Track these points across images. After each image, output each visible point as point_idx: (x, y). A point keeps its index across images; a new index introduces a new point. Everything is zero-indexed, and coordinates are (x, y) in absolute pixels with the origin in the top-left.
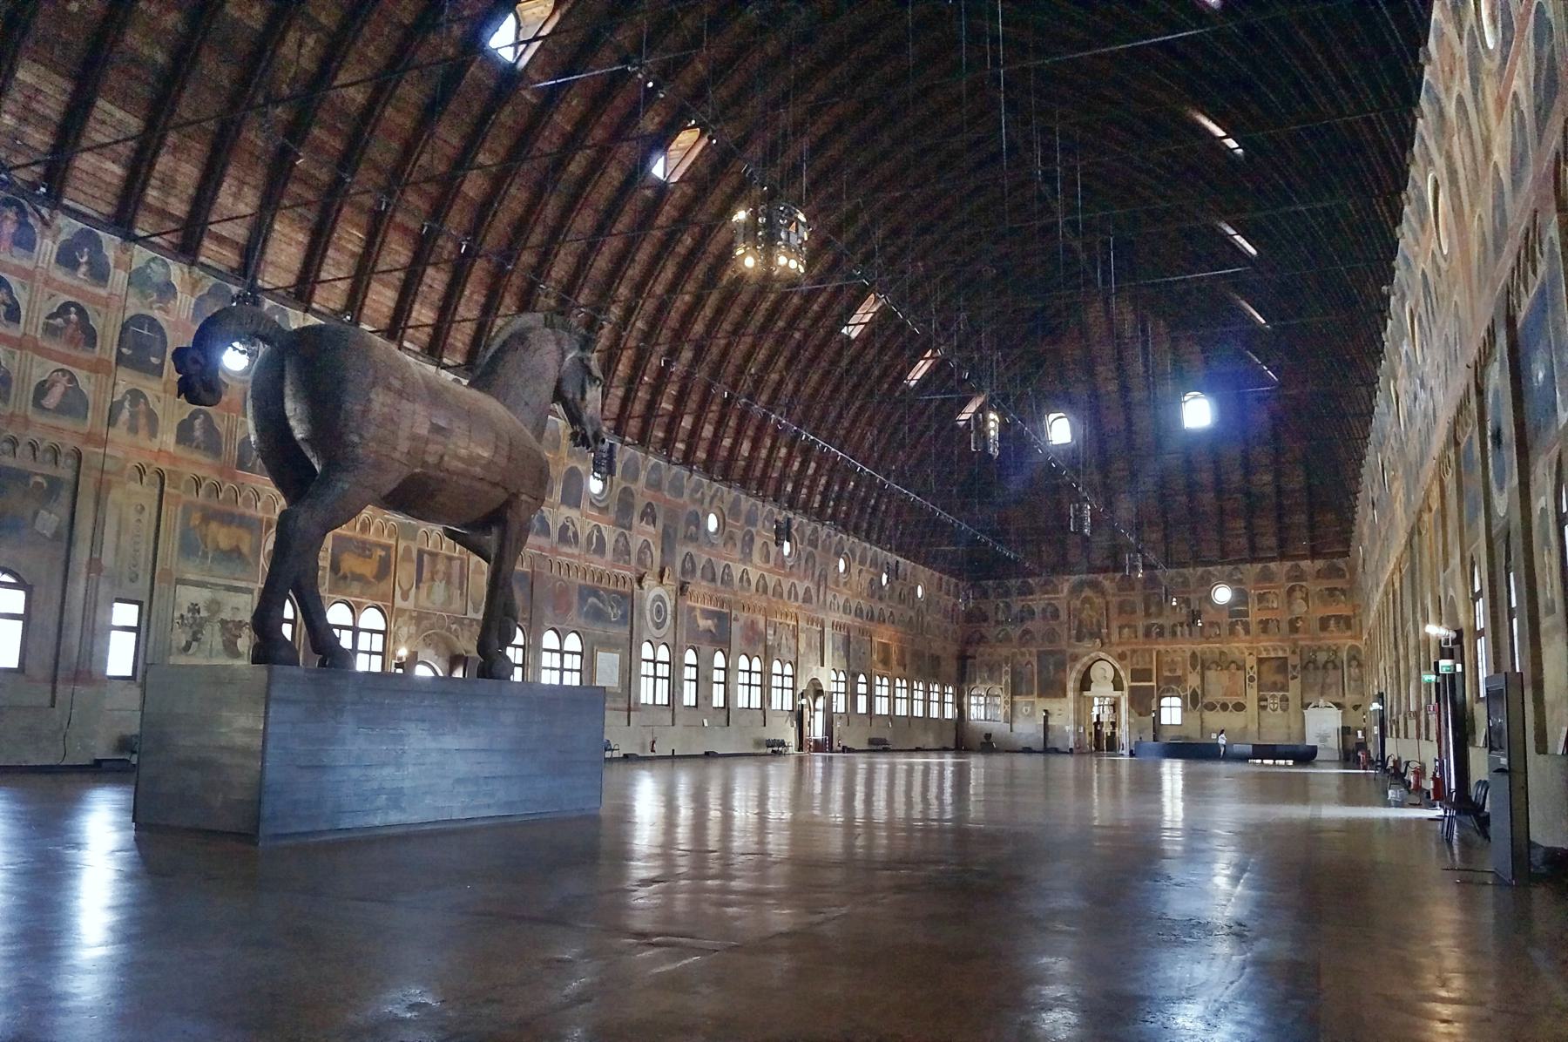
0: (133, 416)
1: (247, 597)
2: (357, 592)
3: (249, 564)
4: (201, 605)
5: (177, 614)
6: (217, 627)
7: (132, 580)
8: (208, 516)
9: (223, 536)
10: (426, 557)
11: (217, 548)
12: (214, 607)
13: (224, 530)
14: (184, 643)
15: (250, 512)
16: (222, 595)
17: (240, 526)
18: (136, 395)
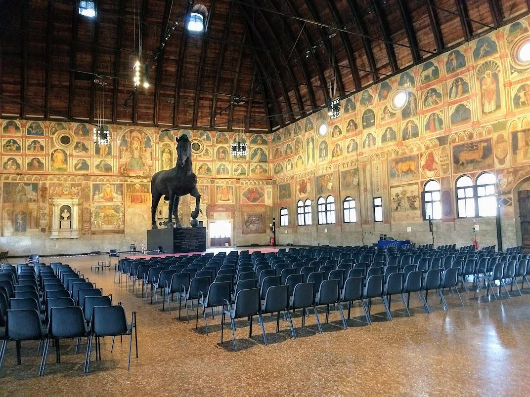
0: (369, 141)
1: (416, 186)
2: (472, 168)
3: (415, 173)
4: (400, 193)
5: (392, 198)
6: (406, 200)
7: (377, 191)
8: (397, 162)
9: (403, 167)
10: (519, 135)
11: (403, 171)
12: (404, 193)
13: (404, 164)
14: (395, 208)
15: (413, 154)
16: (406, 188)
17: (410, 160)
18: (369, 134)
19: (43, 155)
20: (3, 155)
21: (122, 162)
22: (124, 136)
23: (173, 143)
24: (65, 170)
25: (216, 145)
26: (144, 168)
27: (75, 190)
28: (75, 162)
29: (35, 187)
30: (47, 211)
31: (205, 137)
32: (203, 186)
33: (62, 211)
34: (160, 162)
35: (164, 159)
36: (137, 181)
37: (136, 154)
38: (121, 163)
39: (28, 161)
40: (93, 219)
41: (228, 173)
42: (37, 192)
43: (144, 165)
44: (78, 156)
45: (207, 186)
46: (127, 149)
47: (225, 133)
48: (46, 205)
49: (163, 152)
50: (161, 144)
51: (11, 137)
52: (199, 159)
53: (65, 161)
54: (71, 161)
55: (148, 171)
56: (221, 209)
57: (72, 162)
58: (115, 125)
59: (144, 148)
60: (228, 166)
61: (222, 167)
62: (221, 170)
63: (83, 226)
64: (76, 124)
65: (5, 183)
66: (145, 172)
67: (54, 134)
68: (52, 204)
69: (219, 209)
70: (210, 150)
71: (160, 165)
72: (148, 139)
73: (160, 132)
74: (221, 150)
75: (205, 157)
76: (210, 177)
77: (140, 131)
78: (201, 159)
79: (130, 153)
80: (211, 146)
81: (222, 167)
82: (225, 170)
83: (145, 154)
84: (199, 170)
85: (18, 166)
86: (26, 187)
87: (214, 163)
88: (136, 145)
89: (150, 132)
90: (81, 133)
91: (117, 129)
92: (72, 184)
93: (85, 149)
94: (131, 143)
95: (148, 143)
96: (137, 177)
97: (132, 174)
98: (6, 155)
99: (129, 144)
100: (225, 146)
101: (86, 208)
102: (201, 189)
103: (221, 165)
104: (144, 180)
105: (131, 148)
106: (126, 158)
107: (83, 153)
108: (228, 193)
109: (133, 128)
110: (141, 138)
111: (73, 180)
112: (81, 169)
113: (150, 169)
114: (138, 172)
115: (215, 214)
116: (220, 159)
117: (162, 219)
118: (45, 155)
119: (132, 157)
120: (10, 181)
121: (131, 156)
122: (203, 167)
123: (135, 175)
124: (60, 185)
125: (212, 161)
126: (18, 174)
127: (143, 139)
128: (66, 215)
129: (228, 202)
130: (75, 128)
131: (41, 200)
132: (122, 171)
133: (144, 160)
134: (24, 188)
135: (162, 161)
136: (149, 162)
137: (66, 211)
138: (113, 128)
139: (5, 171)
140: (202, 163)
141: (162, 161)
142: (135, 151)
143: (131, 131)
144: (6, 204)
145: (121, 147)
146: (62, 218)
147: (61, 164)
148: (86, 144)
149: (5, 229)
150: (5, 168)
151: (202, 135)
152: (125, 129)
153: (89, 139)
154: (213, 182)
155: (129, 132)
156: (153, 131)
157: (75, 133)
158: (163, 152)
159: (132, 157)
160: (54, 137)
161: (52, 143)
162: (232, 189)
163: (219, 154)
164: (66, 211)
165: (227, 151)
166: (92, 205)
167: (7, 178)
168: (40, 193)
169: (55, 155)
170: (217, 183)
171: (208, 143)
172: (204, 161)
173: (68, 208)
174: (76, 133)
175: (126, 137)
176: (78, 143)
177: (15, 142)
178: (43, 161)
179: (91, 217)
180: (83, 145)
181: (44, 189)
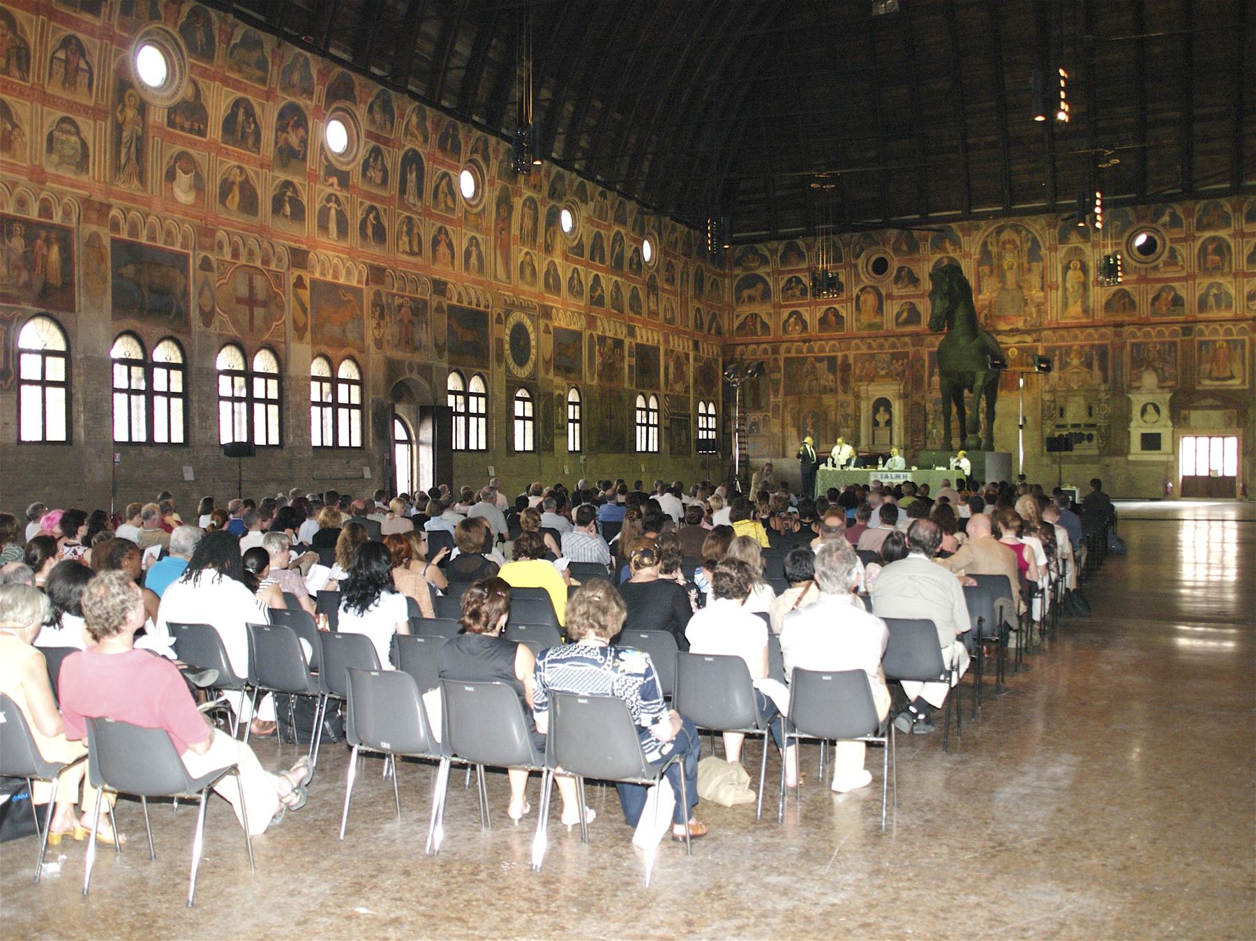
19: (842, 301)
20: (782, 307)
22: (985, 244)
23: (1089, 245)
24: (879, 327)
25: (1198, 234)
27: (898, 366)
28: (896, 309)
29: (832, 360)
30: (851, 410)
31: (1166, 218)
32: (1163, 343)
33: (876, 410)
35: (1069, 285)
36: (1010, 341)
37: (1011, 277)
39: (819, 314)
40: (929, 426)
41: (1229, 306)
42: (835, 374)
43: (1026, 304)
44: (902, 297)
45: (1173, 344)
46: (992, 272)
47: (1222, 201)
48: (850, 398)
49: (1066, 268)
50: (1063, 250)
51: (792, 271)
52: (1152, 275)
53: (879, 310)
54: (889, 309)
56: (1210, 401)
57: (892, 309)
58: (966, 223)
59: (1026, 265)
60: (1229, 285)
61: (1214, 291)
62: (1211, 300)
63: (912, 441)
64: (895, 232)
65: (786, 359)
67: (858, 256)
68: (857, 397)
69: (1203, 403)
70: (1183, 250)
71: (1060, 299)
72: (1036, 244)
73: (1060, 223)
74: (1210, 248)
75: (1168, 269)
76: (1181, 318)
77: (1016, 229)
78: (1159, 276)
80: (1185, 240)
81: (1214, 291)
82: (1223, 300)
83: (1027, 277)
84: (1153, 304)
85: (804, 323)
86: (817, 365)
87: (1191, 282)
88: (1009, 259)
89: (1038, 227)
90: (904, 248)
91: (969, 229)
92: (892, 354)
93: (914, 281)
94: (1000, 257)
95: (1034, 254)
96: (1011, 330)
97: (1003, 326)
98: (786, 306)
100: (1223, 233)
101: (917, 404)
102: (1159, 352)
103: (1211, 286)
104: (1028, 339)
105: (1000, 267)
107: (910, 290)
108: (1230, 359)
109: (1002, 222)
110: (1018, 243)
111: (893, 346)
112: (907, 322)
113: (1039, 311)
114: (1014, 319)
115: (1196, 416)
116: (1207, 271)
117: (1064, 426)
118: (845, 301)
119: (1003, 288)
120: (793, 354)
121: (1000, 285)
122: (1164, 295)
123: (1007, 328)
124: (873, 356)
125: (1185, 279)
126: (805, 341)
128: (882, 417)
129: (1230, 382)
130: (893, 240)
131: (840, 390)
133: (1026, 292)
134: (814, 367)
135: (1065, 290)
136: (1037, 294)
137: (882, 409)
138: (962, 230)
139: (787, 337)
140: (1159, 286)
141: (1065, 290)
143: (999, 231)
144: (789, 398)
146: (876, 423)
147: (872, 314)
148: (915, 268)
149: (788, 443)
150: (785, 330)
151: (1157, 215)
152: (985, 230)
153: (919, 260)
154: (1187, 331)
157: (894, 251)
158: (1066, 268)
159: (1003, 288)
160: (861, 262)
161: (857, 274)
162: (1243, 347)
163: (1205, 256)
164: (882, 409)
165: (1229, 248)
166: (928, 396)
167: (789, 351)
168: (839, 375)
169: (862, 298)
170: (1201, 333)
171: (1177, 233)
172: (1167, 280)
173: (883, 404)
174: (897, 250)
176: (900, 270)
177: (799, 281)
178: (843, 313)
179: (926, 420)
180: (910, 272)
181: (846, 367)
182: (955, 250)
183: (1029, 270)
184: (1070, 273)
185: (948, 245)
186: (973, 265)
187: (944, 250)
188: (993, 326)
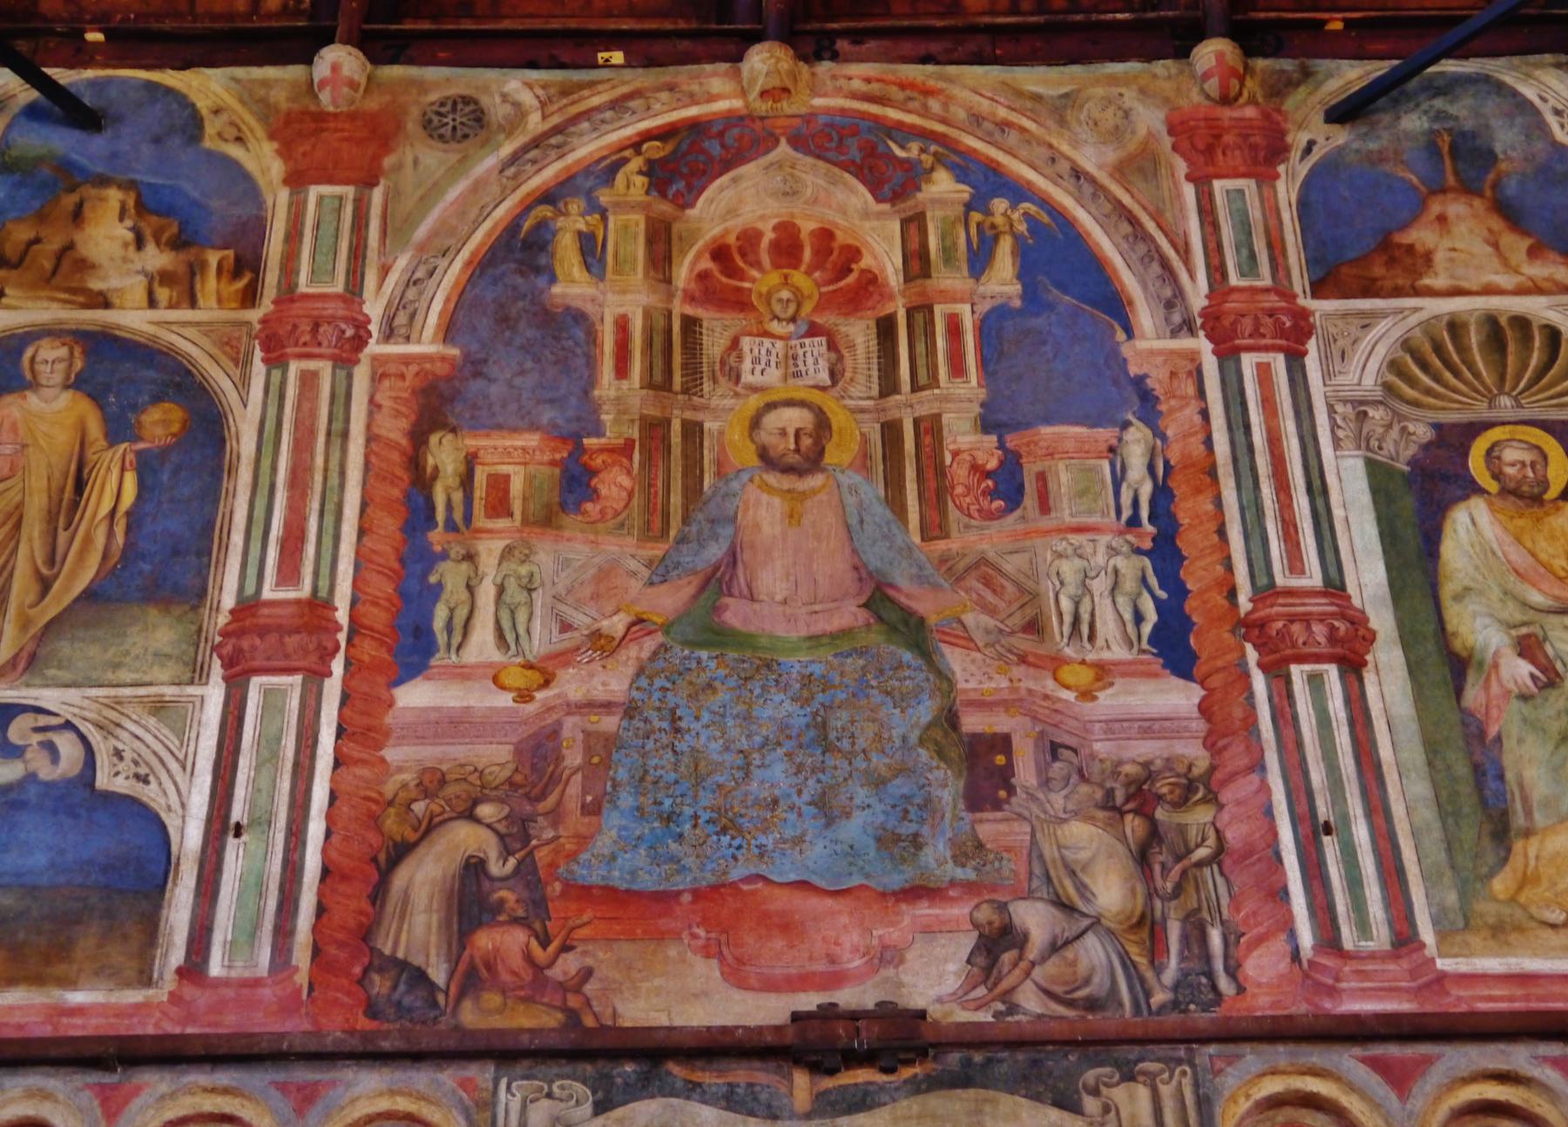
21: (454, 725)
22: (522, 249)
26: (990, 828)
34: (1389, 681)
35: (1479, 627)
38: (404, 758)
46: (576, 482)
50: (1363, 344)
55: (1111, 892)
59: (964, 437)
66: (1035, 919)
73: (1312, 135)
79: (629, 554)
94: (676, 357)
99: (619, 396)
106: (540, 639)
109: (714, 92)
110: (884, 253)
114: (844, 934)
121: (668, 600)
123: (764, 1011)
127: (949, 279)
132: (417, 927)
135: (1445, 666)
141: (1445, 666)
142: (763, 509)
143: (684, 162)
145: (444, 454)
155: (632, 182)
156: (1150, 120)
175: (566, 249)
182: (182, 286)
183: (1007, 485)
184: (1471, 531)
185: (106, 235)
186: (367, 408)
187: (68, 273)
188: (537, 982)
